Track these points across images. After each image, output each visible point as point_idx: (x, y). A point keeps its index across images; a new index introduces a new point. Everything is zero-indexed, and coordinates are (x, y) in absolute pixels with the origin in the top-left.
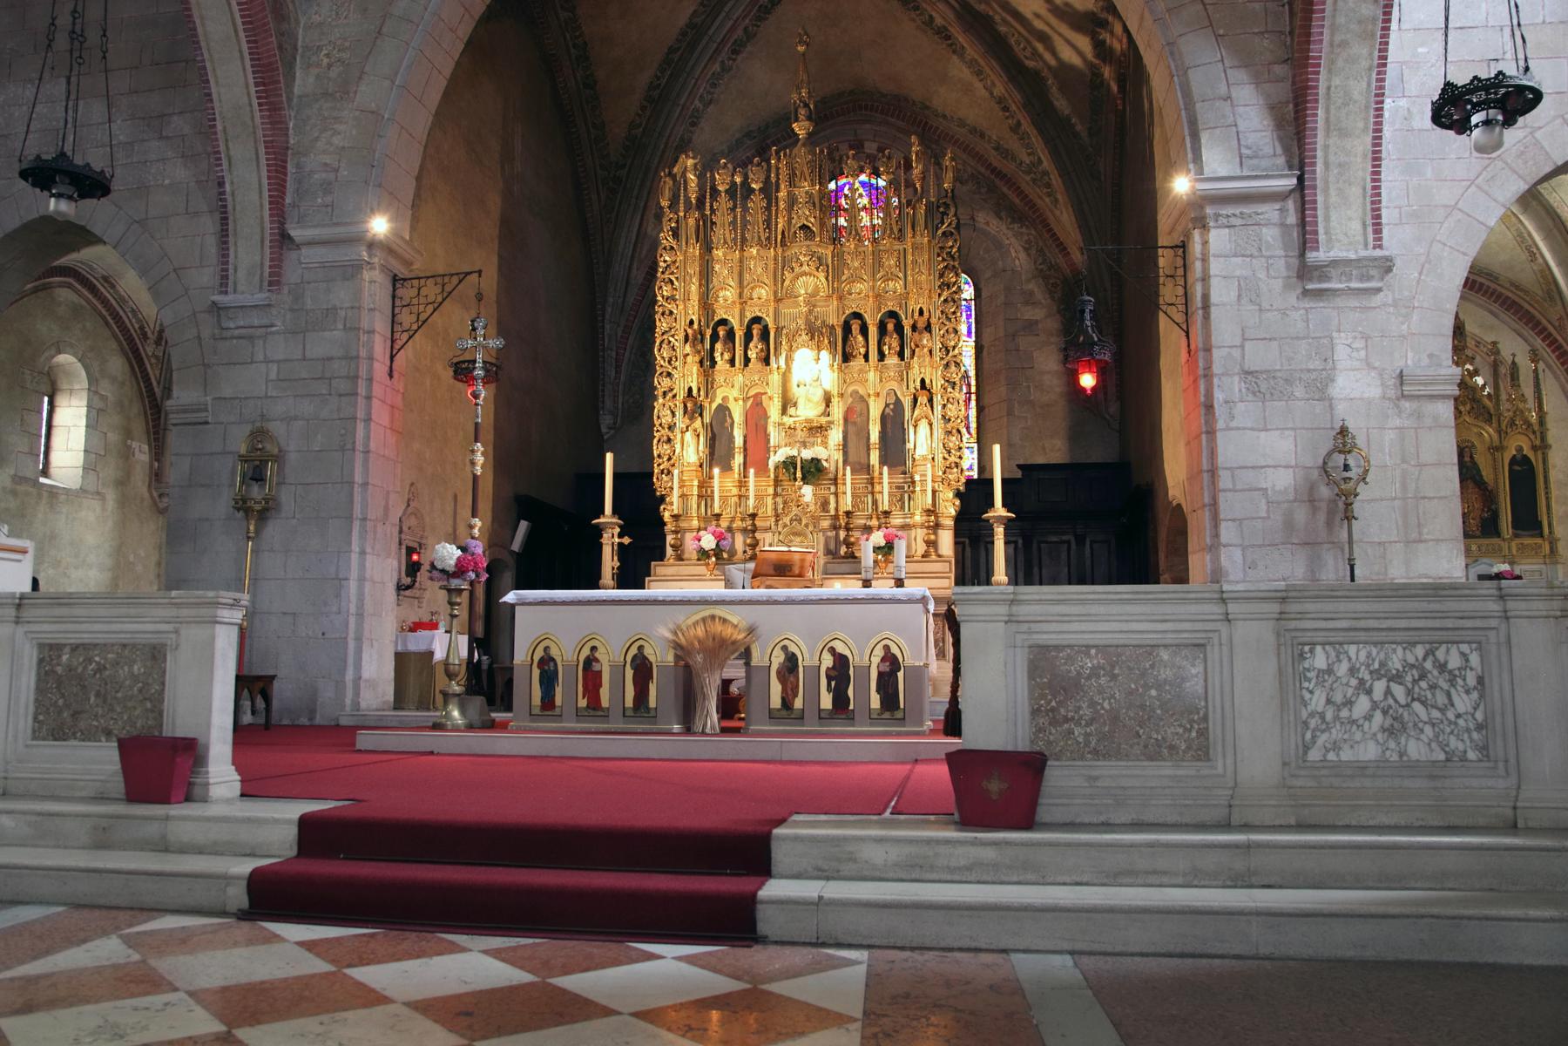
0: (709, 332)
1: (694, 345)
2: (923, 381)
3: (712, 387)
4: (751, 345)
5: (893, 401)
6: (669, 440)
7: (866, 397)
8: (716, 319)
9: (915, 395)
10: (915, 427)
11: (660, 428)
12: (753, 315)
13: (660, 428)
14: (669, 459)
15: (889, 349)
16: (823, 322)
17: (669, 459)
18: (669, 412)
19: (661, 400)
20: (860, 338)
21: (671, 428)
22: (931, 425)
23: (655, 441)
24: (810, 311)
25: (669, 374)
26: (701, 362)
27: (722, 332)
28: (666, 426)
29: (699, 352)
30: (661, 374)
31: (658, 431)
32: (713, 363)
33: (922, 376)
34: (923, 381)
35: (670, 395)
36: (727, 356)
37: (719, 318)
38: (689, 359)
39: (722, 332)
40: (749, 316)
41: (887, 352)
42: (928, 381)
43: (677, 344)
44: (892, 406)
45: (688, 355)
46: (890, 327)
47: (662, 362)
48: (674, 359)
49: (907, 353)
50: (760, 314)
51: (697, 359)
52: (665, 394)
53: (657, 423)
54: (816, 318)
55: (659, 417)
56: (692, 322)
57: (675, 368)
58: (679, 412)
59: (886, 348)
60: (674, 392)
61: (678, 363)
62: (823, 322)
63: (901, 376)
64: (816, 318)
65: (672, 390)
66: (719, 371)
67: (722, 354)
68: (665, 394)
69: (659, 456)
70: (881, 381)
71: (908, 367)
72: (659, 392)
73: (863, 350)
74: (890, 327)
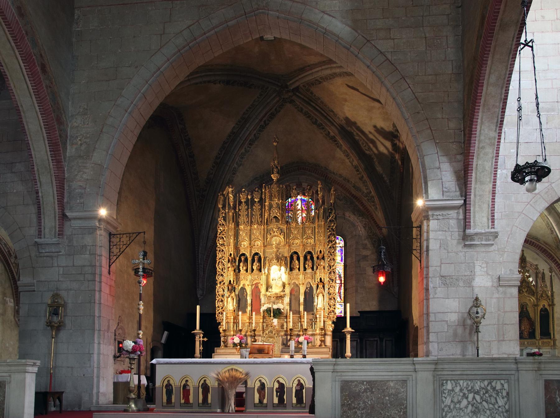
0: (238, 259)
1: (232, 264)
2: (321, 279)
3: (239, 280)
4: (254, 264)
5: (309, 287)
6: (222, 301)
7: (299, 285)
8: (240, 253)
9: (317, 284)
10: (318, 296)
11: (218, 296)
12: (255, 252)
13: (218, 296)
14: (222, 308)
15: (308, 266)
16: (283, 255)
17: (222, 308)
18: (222, 290)
19: (219, 285)
20: (297, 262)
21: (223, 296)
22: (323, 296)
23: (217, 301)
24: (278, 251)
25: (222, 275)
26: (235, 270)
27: (243, 259)
28: (221, 295)
29: (234, 266)
30: (219, 275)
31: (218, 297)
32: (239, 271)
33: (320, 277)
34: (321, 279)
35: (222, 283)
36: (245, 268)
37: (242, 253)
38: (230, 269)
39: (243, 259)
40: (253, 252)
41: (307, 267)
42: (322, 279)
43: (225, 263)
44: (309, 289)
45: (229, 267)
46: (309, 257)
47: (219, 270)
48: (224, 269)
49: (315, 268)
50: (258, 252)
51: (233, 269)
52: (220, 283)
53: (217, 294)
54: (280, 254)
55: (218, 292)
56: (231, 254)
57: (224, 272)
58: (226, 290)
59: (307, 266)
60: (224, 282)
61: (225, 271)
62: (283, 255)
63: (312, 277)
64: (280, 254)
65: (223, 281)
66: (242, 274)
67: (243, 267)
68: (220, 283)
69: (218, 307)
70: (305, 279)
71: (315, 273)
72: (218, 282)
73: (298, 267)
74: (309, 257)
